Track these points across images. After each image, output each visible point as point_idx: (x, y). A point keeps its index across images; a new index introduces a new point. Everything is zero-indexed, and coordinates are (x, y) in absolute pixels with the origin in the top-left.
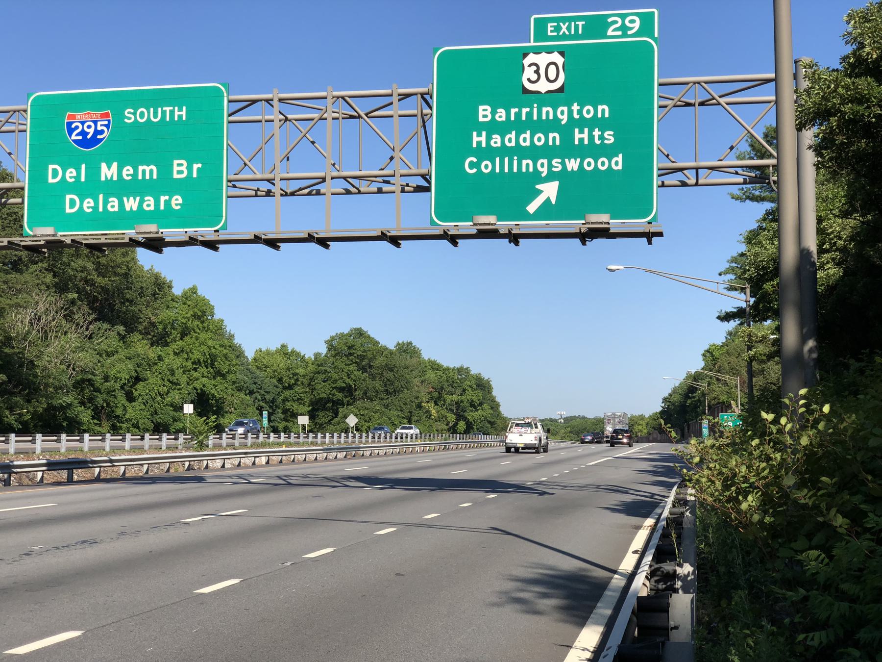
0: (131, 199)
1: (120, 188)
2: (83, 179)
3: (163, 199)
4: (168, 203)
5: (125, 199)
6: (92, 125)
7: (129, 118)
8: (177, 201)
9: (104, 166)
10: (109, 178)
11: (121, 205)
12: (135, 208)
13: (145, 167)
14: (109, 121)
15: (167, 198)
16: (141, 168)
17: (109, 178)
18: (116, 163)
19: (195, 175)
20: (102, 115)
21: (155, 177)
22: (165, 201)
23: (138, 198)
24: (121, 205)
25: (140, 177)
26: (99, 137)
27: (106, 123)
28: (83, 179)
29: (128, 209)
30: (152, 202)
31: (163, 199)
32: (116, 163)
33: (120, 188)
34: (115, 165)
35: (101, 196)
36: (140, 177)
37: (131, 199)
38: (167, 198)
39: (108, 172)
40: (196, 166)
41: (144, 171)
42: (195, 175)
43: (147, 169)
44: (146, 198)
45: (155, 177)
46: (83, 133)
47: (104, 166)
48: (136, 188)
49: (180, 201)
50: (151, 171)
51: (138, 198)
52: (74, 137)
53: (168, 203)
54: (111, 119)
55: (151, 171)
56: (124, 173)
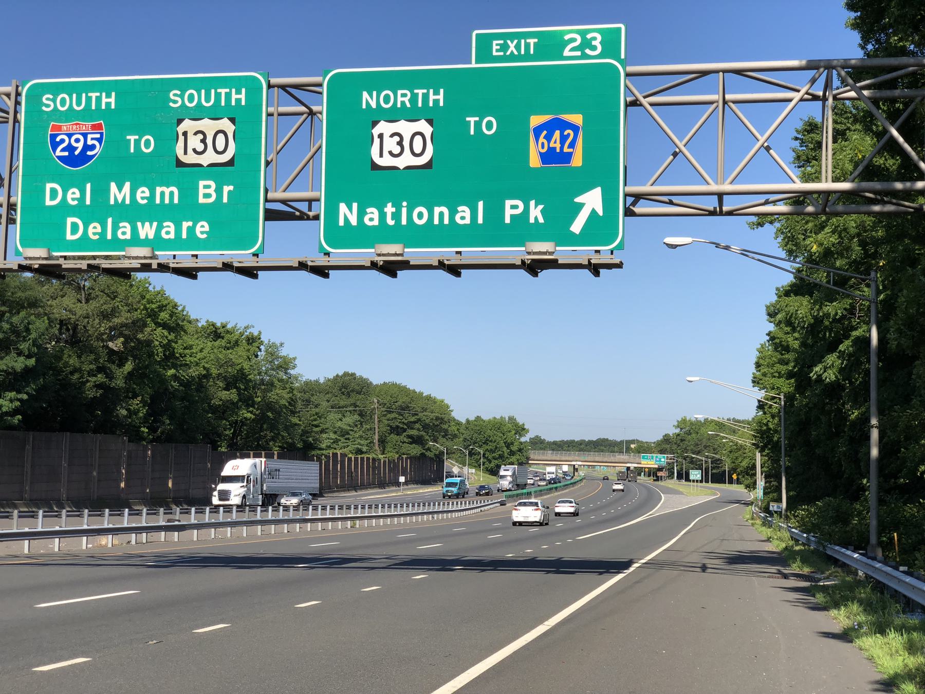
0: (147, 224)
2: (88, 202)
3: (186, 225)
5: (139, 224)
6: (81, 138)
10: (120, 201)
11: (134, 230)
12: (151, 236)
13: (164, 189)
14: (102, 134)
15: (190, 224)
16: (159, 190)
17: (120, 201)
18: (129, 183)
19: (225, 200)
20: (94, 127)
21: (176, 201)
22: (188, 228)
23: (155, 224)
25: (158, 201)
26: (89, 153)
27: (98, 136)
28: (88, 202)
30: (172, 229)
31: (186, 225)
32: (129, 183)
34: (127, 186)
35: (110, 221)
36: (158, 201)
37: (147, 224)
38: (190, 224)
40: (227, 189)
42: (225, 200)
43: (167, 191)
44: (165, 224)
45: (176, 201)
46: (70, 148)
49: (207, 228)
50: (172, 194)
51: (155, 224)
52: (58, 153)
53: (191, 230)
54: (104, 131)
55: (172, 194)
56: (139, 195)
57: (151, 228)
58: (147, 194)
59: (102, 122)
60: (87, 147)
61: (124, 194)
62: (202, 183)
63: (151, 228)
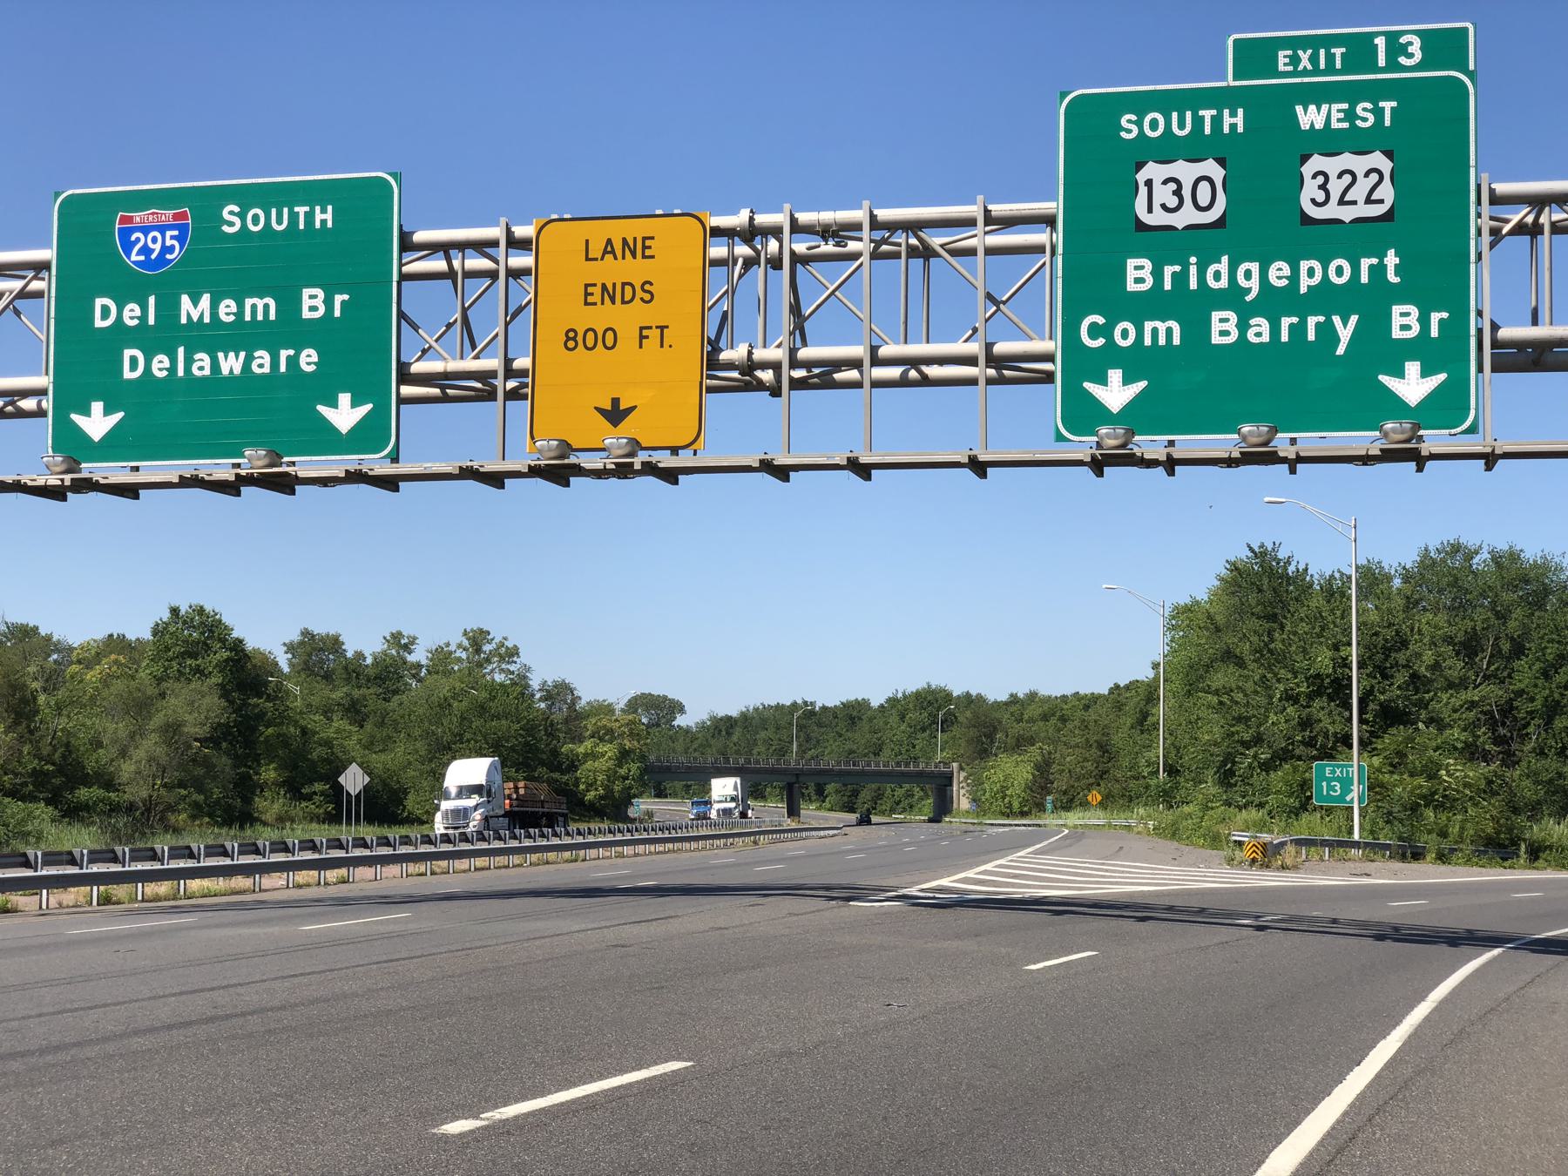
0: (232, 355)
1: (212, 337)
2: (151, 321)
3: (284, 354)
4: (293, 362)
5: (221, 355)
8: (308, 359)
9: (185, 300)
10: (195, 320)
11: (215, 366)
12: (237, 370)
15: (291, 352)
16: (249, 302)
17: (195, 320)
18: (209, 295)
19: (337, 313)
21: (272, 316)
22: (288, 357)
23: (242, 354)
24: (215, 366)
25: (248, 318)
28: (151, 321)
29: (225, 371)
31: (284, 354)
33: (212, 337)
34: (205, 301)
35: (181, 350)
36: (248, 318)
37: (232, 355)
38: (291, 352)
39: (192, 309)
42: (337, 313)
43: (260, 303)
44: (257, 354)
45: (272, 316)
47: (185, 300)
48: (243, 336)
49: (315, 358)
50: (266, 306)
51: (242, 354)
53: (293, 362)
55: (266, 306)
56: (222, 310)
57: (237, 359)
58: (234, 309)
61: (186, 312)
62: (306, 292)
63: (237, 359)
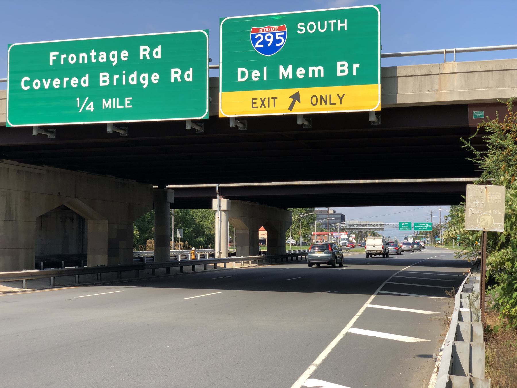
2: (265, 78)
7: (302, 30)
9: (281, 68)
10: (286, 77)
13: (314, 68)
14: (285, 32)
16: (311, 69)
17: (286, 77)
19: (355, 73)
21: (322, 75)
25: (310, 76)
26: (277, 45)
27: (283, 34)
28: (265, 78)
32: (291, 65)
34: (290, 67)
36: (310, 76)
41: (313, 71)
42: (355, 73)
43: (316, 69)
45: (322, 75)
46: (265, 42)
47: (281, 68)
50: (319, 71)
52: (257, 46)
54: (286, 31)
55: (319, 71)
56: (298, 73)
59: (285, 25)
60: (275, 41)
62: (339, 63)
